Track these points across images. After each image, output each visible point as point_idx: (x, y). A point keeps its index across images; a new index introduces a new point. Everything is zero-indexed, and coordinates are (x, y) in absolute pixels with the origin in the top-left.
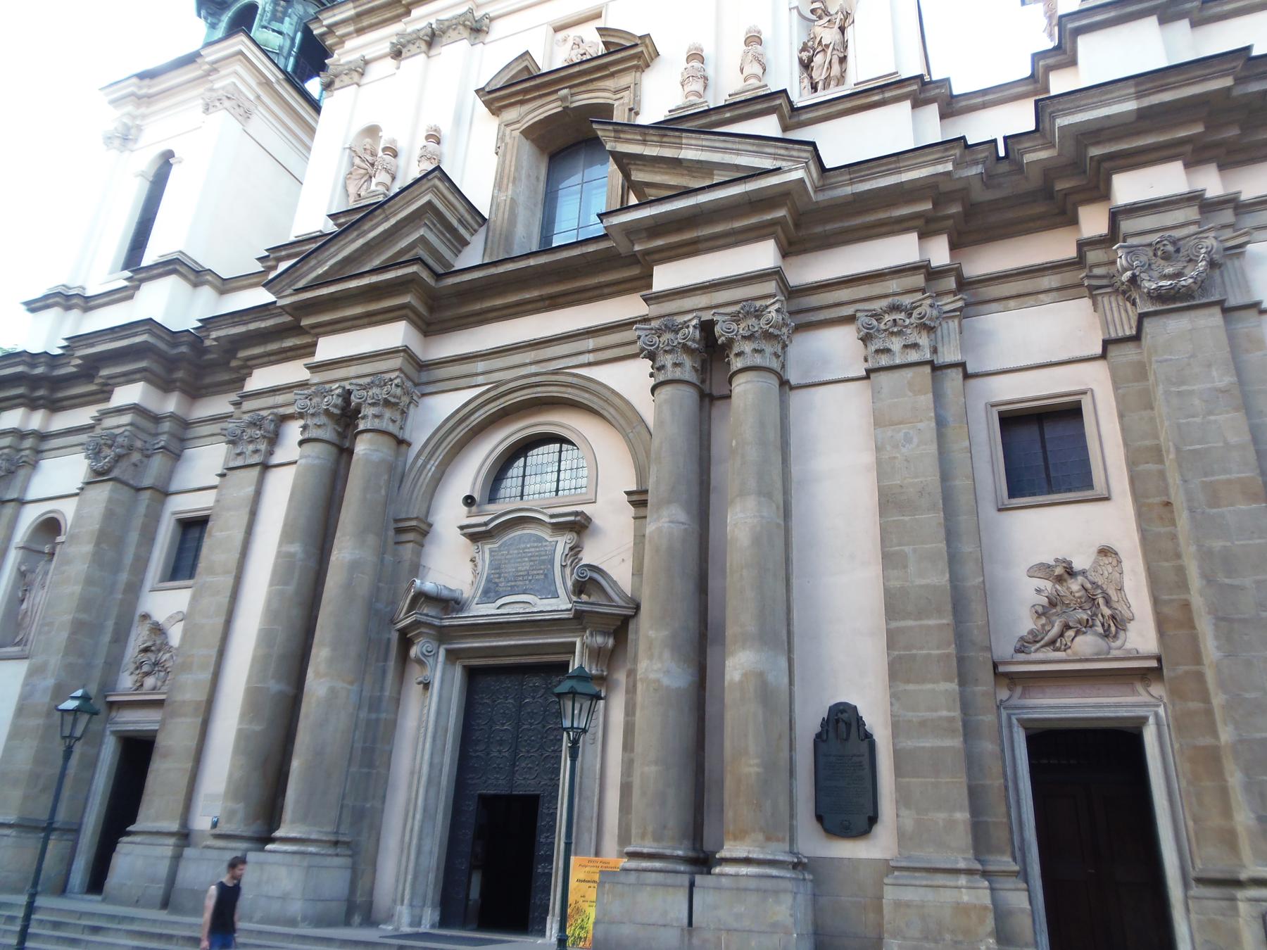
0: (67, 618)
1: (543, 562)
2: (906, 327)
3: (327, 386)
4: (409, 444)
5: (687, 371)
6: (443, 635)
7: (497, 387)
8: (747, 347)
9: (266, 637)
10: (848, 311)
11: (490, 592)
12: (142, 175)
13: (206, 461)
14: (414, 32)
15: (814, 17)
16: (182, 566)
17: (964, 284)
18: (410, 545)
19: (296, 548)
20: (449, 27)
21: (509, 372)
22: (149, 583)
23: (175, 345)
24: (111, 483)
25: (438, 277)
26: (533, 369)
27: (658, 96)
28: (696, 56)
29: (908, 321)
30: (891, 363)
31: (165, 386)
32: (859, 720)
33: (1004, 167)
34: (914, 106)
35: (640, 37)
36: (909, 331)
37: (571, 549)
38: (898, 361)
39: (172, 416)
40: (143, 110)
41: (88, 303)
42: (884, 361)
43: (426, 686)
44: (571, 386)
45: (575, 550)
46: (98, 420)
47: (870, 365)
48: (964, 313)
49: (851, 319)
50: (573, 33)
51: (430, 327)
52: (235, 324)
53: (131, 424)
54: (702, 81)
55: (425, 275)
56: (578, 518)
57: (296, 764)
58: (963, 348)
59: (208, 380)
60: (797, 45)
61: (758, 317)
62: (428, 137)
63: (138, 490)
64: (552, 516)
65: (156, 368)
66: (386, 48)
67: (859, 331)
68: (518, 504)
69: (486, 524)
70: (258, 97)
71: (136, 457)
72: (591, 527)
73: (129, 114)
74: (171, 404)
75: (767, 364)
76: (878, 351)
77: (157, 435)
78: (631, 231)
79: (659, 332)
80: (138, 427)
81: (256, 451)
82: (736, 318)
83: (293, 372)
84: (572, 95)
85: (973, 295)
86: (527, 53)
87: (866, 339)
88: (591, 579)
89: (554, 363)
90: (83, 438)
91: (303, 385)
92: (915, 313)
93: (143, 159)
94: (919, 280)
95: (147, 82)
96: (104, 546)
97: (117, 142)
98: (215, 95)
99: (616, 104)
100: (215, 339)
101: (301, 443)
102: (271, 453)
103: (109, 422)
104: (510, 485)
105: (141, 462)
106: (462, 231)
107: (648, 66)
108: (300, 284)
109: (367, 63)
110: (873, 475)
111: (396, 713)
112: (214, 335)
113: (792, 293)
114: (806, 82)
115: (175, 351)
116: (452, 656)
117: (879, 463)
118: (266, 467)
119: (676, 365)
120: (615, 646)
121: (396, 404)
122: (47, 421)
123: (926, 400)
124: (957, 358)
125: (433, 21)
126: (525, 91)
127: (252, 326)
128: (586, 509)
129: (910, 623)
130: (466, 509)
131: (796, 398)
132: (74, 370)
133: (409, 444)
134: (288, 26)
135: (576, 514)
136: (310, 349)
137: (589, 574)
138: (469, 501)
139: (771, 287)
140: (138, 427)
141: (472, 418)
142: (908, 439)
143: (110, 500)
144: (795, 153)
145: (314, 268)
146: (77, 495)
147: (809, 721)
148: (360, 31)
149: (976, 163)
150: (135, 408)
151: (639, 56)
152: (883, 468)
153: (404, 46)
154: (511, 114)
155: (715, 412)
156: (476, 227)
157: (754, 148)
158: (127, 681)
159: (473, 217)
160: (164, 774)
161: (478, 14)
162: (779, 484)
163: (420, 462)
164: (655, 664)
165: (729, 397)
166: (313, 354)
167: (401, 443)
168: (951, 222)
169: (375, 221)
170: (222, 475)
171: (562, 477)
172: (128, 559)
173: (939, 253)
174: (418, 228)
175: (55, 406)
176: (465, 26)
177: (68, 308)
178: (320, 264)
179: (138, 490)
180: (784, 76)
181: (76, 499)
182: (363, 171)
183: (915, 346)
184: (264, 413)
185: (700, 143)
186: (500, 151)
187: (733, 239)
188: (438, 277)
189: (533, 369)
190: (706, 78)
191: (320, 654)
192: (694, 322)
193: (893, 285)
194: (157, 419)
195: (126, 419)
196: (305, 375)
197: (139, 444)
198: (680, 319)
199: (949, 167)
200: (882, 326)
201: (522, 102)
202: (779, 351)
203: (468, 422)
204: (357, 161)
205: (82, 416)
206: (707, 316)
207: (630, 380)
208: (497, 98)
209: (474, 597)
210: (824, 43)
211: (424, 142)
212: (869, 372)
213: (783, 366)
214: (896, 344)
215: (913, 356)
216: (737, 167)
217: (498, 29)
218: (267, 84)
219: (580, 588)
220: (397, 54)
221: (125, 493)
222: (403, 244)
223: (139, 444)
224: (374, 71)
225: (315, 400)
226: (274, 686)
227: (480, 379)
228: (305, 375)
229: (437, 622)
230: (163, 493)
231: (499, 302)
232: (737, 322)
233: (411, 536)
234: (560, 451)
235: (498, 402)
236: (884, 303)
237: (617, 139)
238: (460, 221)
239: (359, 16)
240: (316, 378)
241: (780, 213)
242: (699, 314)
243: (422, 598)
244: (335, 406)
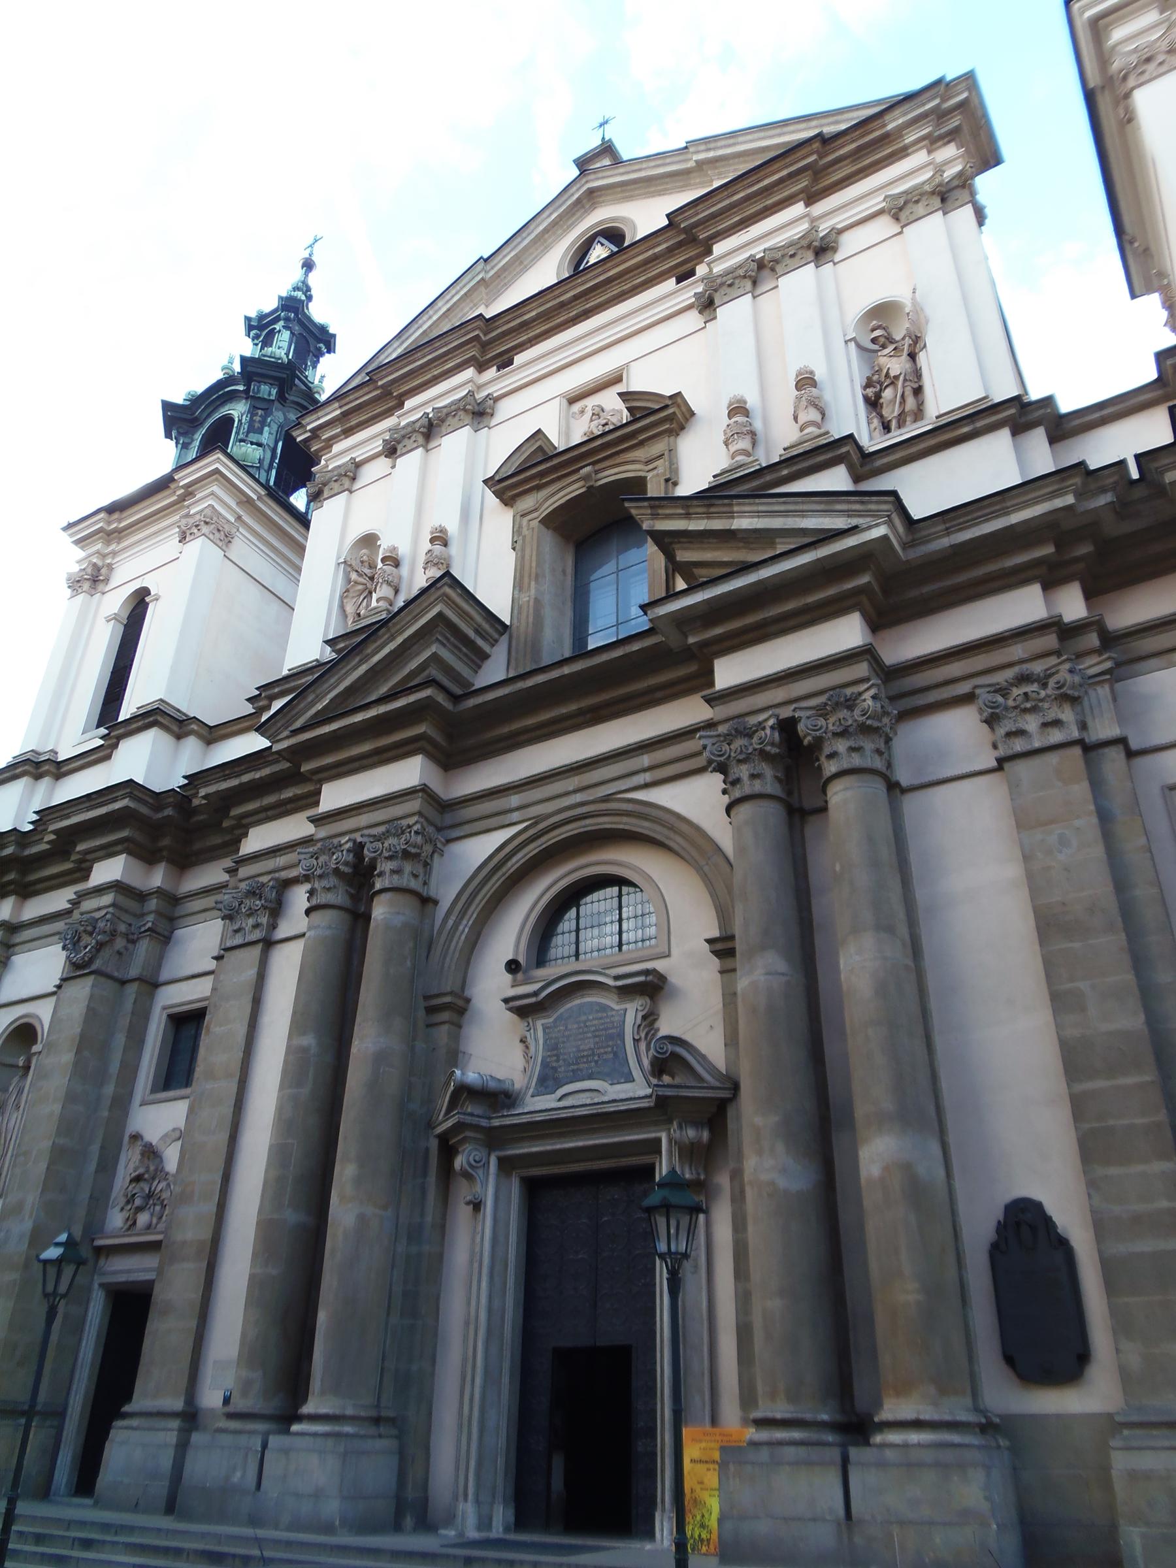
0: (46, 1144)
1: (611, 1037)
2: (1042, 700)
3: (335, 841)
4: (436, 902)
5: (769, 784)
6: (494, 1138)
7: (536, 823)
8: (841, 746)
9: (279, 1154)
10: (964, 688)
11: (548, 1080)
12: (115, 618)
13: (201, 940)
14: (408, 425)
15: (876, 347)
16: (177, 1072)
17: (1109, 640)
18: (446, 1027)
19: (308, 1040)
20: (447, 415)
21: (547, 804)
22: (138, 1097)
23: (158, 808)
24: (92, 977)
25: (456, 699)
26: (578, 798)
27: (699, 462)
28: (738, 409)
29: (1043, 693)
30: (1029, 748)
31: (147, 856)
32: (1048, 1222)
33: (1139, 493)
34: (1014, 434)
35: (671, 397)
36: (1046, 705)
37: (644, 1018)
38: (1037, 744)
39: (159, 892)
40: (113, 547)
41: (58, 769)
42: (1019, 745)
43: (477, 1206)
44: (628, 814)
45: (650, 1019)
46: (75, 903)
47: (1001, 752)
48: (1117, 674)
49: (968, 698)
50: (590, 402)
51: (451, 758)
52: (226, 778)
53: (113, 905)
54: (748, 438)
55: (441, 698)
56: (650, 978)
57: (322, 1316)
58: (1121, 719)
59: (198, 846)
60: (859, 382)
61: (851, 708)
62: (432, 540)
63: (123, 983)
64: (617, 978)
65: (138, 837)
66: (377, 446)
67: (981, 711)
68: (573, 966)
69: (535, 994)
70: (239, 518)
71: (120, 943)
72: (666, 988)
73: (98, 552)
74: (157, 878)
75: (867, 763)
76: (1009, 735)
77: (143, 915)
78: (683, 620)
79: (728, 738)
81: (256, 926)
82: (822, 712)
83: (294, 827)
84: (597, 472)
85: (1125, 652)
86: (539, 430)
87: (991, 721)
88: (674, 1055)
89: (603, 787)
90: (60, 926)
91: (307, 841)
92: (1052, 683)
93: (115, 601)
94: (1050, 641)
95: (116, 516)
96: (86, 1053)
97: (86, 586)
98: (191, 521)
99: (649, 475)
100: (204, 797)
101: (308, 912)
102: (273, 926)
103: (88, 905)
104: (562, 943)
105: (126, 949)
106: (480, 642)
107: (682, 428)
108: (298, 724)
109: (358, 465)
110: (1024, 893)
111: (442, 1245)
112: (202, 792)
113: (889, 674)
114: (876, 422)
115: (160, 815)
116: (506, 1165)
117: (1030, 876)
118: (268, 944)
119: (753, 776)
120: (711, 1140)
121: (417, 855)
122: (17, 909)
123: (1081, 790)
124: (1113, 732)
125: (429, 410)
126: (542, 474)
127: (246, 778)
128: (659, 965)
129: (1099, 1084)
130: (509, 977)
131: (910, 804)
132: (48, 847)
133: (436, 902)
134: (266, 437)
135: (647, 972)
136: (313, 798)
137: (670, 1048)
138: (513, 966)
139: (862, 669)
141: (509, 864)
142: (1063, 842)
143: (92, 997)
144: (873, 507)
145: (312, 704)
146: (54, 993)
147: (980, 1226)
148: (348, 432)
149: (1103, 490)
150: (116, 886)
151: (670, 418)
152: (1035, 882)
153: (399, 442)
154: (527, 503)
155: (809, 830)
156: (496, 636)
157: (822, 507)
158: (116, 1219)
159: (492, 626)
160: (164, 1334)
161: (480, 396)
162: (901, 915)
163: (451, 922)
164: (765, 1161)
165: (824, 809)
166: (317, 803)
167: (426, 902)
168: (1081, 566)
169: (379, 643)
170: (218, 958)
171: (625, 926)
172: (114, 1067)
173: (1072, 605)
174: (428, 646)
175: (26, 892)
176: (465, 410)
177: (38, 777)
178: (318, 698)
179: (123, 983)
180: (849, 418)
181: (54, 998)
182: (360, 587)
183: (1057, 723)
184: (264, 879)
185: (755, 508)
186: (518, 546)
187: (807, 617)
188: (456, 699)
189: (578, 798)
190: (753, 434)
191: (345, 1172)
192: (771, 722)
193: (1017, 651)
194: (141, 896)
195: (107, 899)
196: (309, 829)
197: (122, 928)
198: (753, 720)
199: (1070, 499)
200: (1011, 703)
201: (538, 488)
202: (882, 746)
203: (504, 870)
204: (354, 576)
205: (59, 900)
206: (786, 713)
207: (698, 800)
208: (508, 486)
209: (528, 1088)
210: (892, 374)
211: (428, 546)
212: (1001, 763)
213: (889, 766)
214: (1031, 723)
215: (1056, 736)
216: (804, 532)
217: (505, 409)
218: (246, 502)
219: (660, 1067)
220: (391, 451)
222: (413, 665)
223: (122, 928)
224: (369, 472)
225: (322, 859)
226: (292, 1217)
227: (515, 816)
228: (309, 829)
229: (484, 1123)
230: (151, 984)
231: (530, 721)
232: (825, 716)
233: (445, 1016)
234: (620, 896)
235: (539, 842)
236: (1009, 674)
237: (655, 516)
238: (477, 632)
239: (345, 415)
240: (322, 833)
241: (864, 579)
242: (777, 711)
243: (465, 1093)
244: (346, 864)
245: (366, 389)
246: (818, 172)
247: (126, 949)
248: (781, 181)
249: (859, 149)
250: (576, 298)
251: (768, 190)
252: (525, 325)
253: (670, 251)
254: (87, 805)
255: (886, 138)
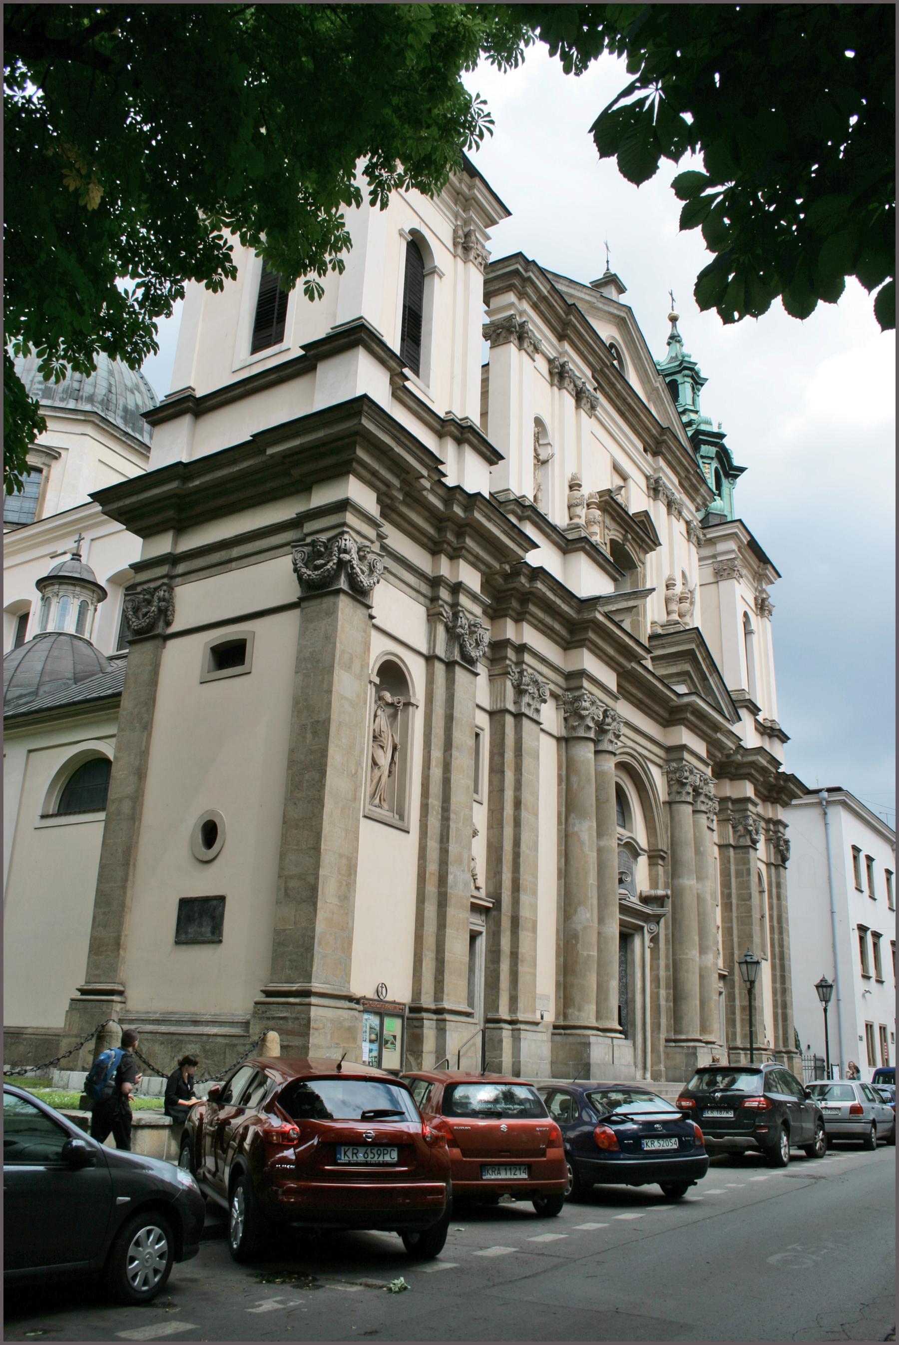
52: (551, 589)
99: (639, 569)
127: (550, 594)
148: (535, 307)
239: (545, 298)
245: (562, 305)
248: (684, 466)
250: (629, 405)
251: (680, 463)
252: (612, 386)
253: (652, 436)
254: (506, 528)
255: (697, 490)
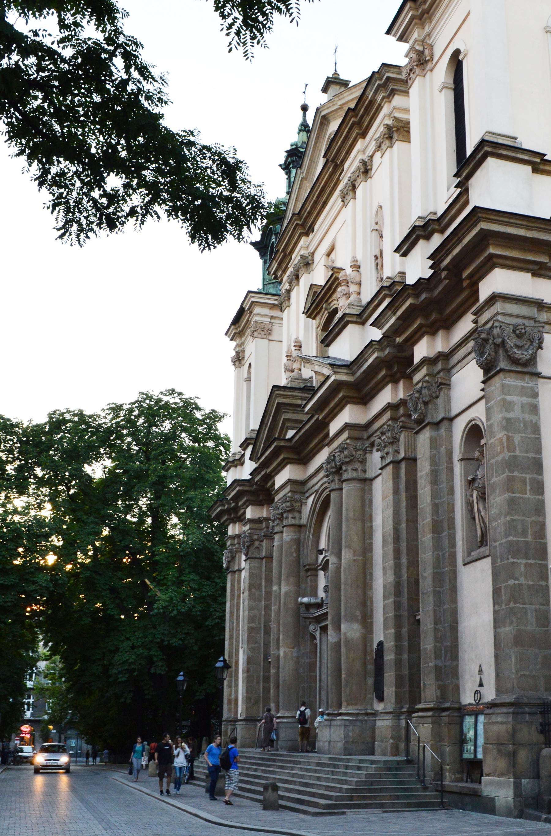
31: (258, 503)
53: (250, 529)
71: (257, 544)
80: (254, 529)
86: (312, 285)
105: (260, 545)
140: (254, 529)
197: (256, 537)
201: (318, 313)
208: (311, 311)
221: (256, 563)
246: (359, 124)
247: (260, 545)
249: (366, 109)
255: (372, 102)
